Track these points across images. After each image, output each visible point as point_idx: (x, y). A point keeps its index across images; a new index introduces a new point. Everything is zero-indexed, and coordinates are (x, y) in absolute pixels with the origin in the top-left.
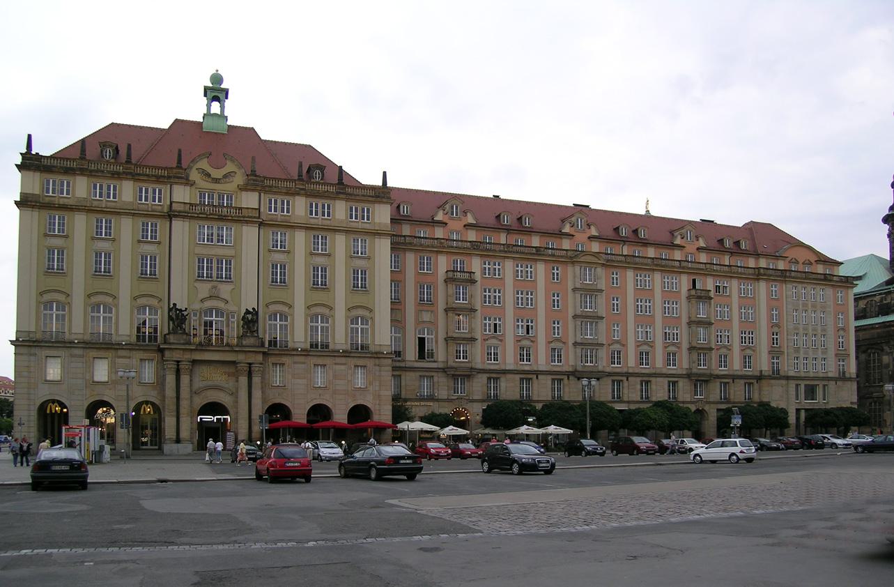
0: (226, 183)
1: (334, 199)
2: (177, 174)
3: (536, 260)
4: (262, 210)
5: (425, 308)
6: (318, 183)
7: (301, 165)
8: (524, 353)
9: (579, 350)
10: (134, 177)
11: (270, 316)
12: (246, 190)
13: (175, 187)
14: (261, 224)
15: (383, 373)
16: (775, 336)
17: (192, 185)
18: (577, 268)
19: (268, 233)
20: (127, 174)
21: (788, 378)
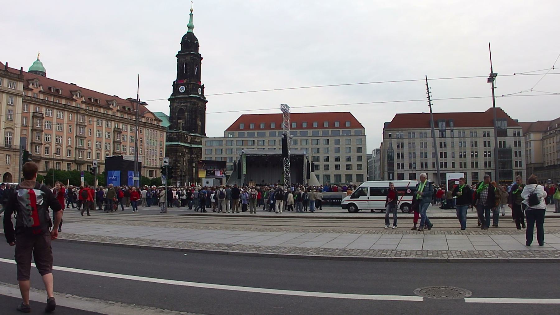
8: (58, 150)
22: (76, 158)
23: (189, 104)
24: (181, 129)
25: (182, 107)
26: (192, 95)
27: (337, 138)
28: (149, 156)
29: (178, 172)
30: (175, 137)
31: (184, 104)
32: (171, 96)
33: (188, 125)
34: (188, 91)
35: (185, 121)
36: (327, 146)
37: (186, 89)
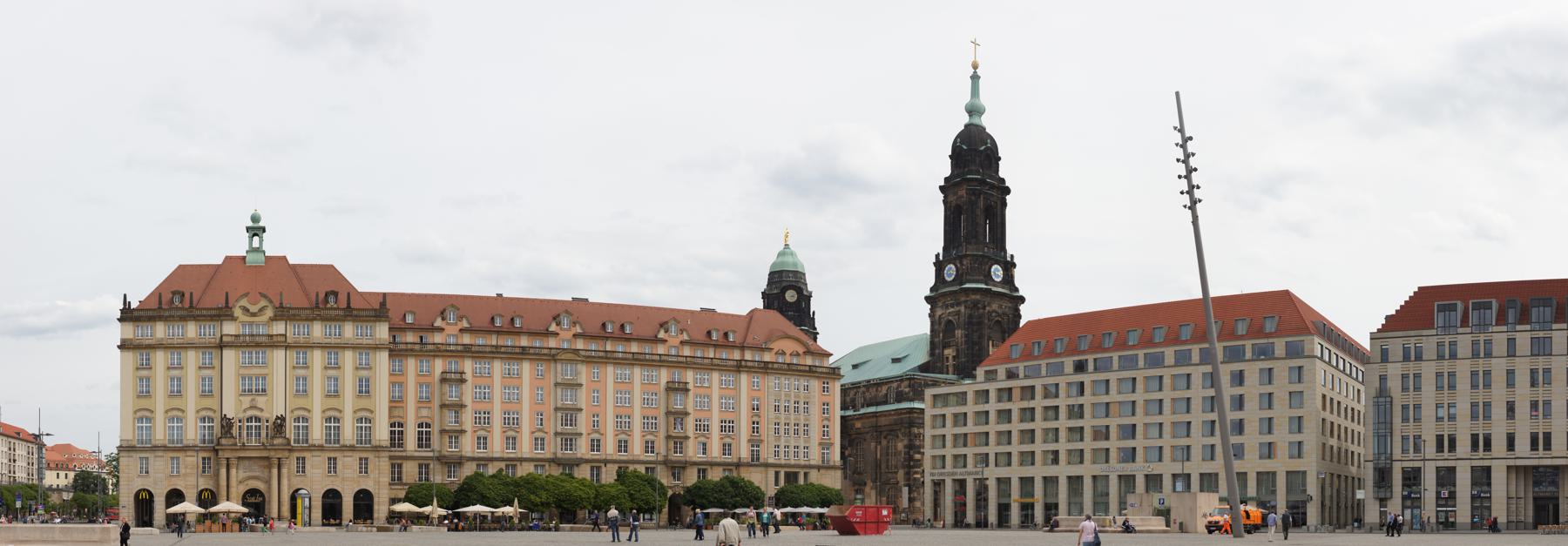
0: (261, 315)
1: (344, 321)
2: (223, 313)
3: (522, 359)
4: (288, 335)
5: (425, 405)
6: (331, 309)
7: (317, 295)
8: (512, 441)
9: (559, 439)
10: (196, 318)
11: (326, 420)
12: (276, 320)
13: (225, 323)
14: (286, 347)
15: (381, 463)
16: (756, 425)
17: (236, 320)
18: (559, 366)
19: (292, 354)
20: (190, 316)
21: (767, 465)
22: (555, 454)
23: (962, 309)
24: (951, 369)
25: (950, 318)
26: (967, 286)
27: (1237, 367)
28: (783, 439)
29: (917, 473)
30: (907, 390)
31: (952, 310)
32: (932, 290)
33: (963, 360)
34: (962, 275)
35: (958, 351)
36: (1269, 389)
37: (957, 271)
